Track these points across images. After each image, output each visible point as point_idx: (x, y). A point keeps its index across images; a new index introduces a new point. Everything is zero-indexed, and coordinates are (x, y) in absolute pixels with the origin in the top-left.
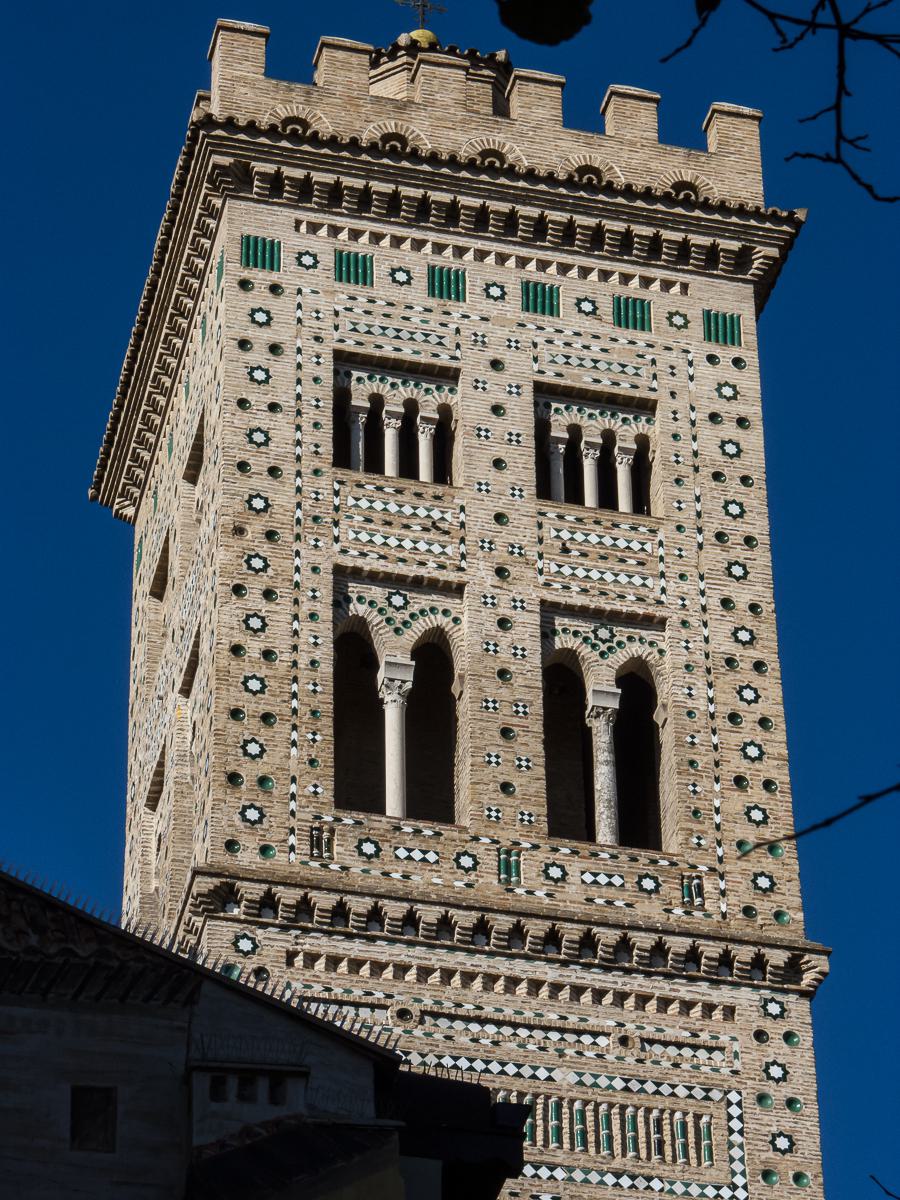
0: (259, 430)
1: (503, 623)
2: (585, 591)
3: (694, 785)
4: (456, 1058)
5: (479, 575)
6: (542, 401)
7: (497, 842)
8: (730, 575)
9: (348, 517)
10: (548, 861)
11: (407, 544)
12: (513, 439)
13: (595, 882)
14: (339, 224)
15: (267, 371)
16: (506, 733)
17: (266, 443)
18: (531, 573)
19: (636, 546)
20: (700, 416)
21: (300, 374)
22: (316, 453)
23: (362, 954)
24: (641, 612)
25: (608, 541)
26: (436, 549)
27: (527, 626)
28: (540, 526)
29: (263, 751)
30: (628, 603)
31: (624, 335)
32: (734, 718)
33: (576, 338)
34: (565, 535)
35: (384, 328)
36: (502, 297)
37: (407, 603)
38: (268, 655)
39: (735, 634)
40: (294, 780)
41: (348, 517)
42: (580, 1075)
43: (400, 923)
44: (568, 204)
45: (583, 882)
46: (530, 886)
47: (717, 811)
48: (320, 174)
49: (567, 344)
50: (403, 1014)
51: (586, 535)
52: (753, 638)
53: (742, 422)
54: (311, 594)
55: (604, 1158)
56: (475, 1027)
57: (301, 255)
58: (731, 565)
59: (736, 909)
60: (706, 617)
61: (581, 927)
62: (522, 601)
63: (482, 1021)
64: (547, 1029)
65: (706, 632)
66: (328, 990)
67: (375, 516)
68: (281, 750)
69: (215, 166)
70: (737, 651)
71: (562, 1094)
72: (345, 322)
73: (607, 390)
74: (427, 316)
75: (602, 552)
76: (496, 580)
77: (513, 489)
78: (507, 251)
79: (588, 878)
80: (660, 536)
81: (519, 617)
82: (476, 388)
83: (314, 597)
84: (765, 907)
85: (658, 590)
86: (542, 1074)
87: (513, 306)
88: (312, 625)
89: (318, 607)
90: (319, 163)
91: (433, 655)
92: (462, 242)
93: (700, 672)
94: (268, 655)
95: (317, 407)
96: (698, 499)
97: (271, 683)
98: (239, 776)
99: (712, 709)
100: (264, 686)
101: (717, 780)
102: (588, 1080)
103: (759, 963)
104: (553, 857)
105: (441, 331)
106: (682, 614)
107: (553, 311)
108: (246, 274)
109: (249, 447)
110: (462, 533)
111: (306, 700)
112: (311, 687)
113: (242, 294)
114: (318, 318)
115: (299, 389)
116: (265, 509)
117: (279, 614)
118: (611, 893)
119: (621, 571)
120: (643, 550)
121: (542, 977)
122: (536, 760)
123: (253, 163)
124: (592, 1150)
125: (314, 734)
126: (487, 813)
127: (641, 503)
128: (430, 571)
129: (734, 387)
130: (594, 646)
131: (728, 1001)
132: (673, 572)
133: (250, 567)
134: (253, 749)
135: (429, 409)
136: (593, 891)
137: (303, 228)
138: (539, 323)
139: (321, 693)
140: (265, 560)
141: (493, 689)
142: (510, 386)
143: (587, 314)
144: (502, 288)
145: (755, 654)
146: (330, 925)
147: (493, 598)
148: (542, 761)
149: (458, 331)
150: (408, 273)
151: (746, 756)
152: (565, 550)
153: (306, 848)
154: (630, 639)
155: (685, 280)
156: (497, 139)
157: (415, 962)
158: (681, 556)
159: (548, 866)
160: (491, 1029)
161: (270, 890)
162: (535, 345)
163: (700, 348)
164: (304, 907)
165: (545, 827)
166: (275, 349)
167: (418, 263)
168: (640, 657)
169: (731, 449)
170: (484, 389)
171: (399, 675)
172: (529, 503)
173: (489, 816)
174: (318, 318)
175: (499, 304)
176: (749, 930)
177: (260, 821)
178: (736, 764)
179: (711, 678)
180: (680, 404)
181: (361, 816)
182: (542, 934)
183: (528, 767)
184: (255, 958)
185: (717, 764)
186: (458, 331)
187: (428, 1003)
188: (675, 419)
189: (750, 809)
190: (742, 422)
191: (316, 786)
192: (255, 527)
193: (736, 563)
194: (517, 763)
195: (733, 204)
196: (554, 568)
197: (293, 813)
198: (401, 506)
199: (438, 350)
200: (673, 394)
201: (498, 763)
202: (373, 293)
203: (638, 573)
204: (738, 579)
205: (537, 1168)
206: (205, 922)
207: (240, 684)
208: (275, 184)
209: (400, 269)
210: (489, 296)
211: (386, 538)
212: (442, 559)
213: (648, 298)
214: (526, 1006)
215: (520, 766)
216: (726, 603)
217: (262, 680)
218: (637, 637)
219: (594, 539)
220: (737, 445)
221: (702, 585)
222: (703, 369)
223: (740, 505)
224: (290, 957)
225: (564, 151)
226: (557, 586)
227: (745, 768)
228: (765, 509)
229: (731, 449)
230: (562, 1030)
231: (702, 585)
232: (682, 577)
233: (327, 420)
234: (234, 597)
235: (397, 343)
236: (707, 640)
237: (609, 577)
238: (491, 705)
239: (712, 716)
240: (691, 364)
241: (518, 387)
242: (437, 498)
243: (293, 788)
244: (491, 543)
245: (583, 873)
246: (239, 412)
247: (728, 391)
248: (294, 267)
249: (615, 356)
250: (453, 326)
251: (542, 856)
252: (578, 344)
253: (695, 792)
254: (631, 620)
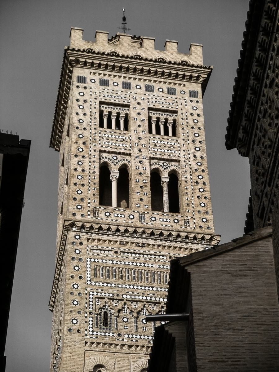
0: (81, 119)
1: (141, 162)
2: (160, 154)
3: (187, 198)
4: (129, 262)
5: (135, 152)
6: (150, 112)
7: (139, 212)
8: (196, 150)
9: (103, 139)
10: (151, 216)
11: (117, 145)
12: (143, 120)
13: (163, 221)
14: (101, 73)
15: (83, 106)
16: (141, 187)
17: (83, 123)
18: (147, 150)
19: (173, 144)
20: (188, 114)
21: (91, 107)
22: (95, 124)
23: (106, 239)
24: (174, 159)
25: (166, 143)
26: (124, 146)
27: (146, 162)
28: (149, 140)
29: (82, 192)
30: (171, 157)
31: (170, 96)
32: (197, 182)
33: (158, 97)
34: (156, 142)
35: (111, 96)
36: (140, 88)
37: (117, 158)
38: (83, 170)
39: (197, 163)
40: (89, 199)
41: (103, 139)
42: (159, 266)
43: (115, 231)
44: (156, 66)
45: (160, 221)
46: (148, 223)
47: (193, 204)
48: (96, 61)
49: (156, 98)
50: (116, 252)
51: (161, 142)
52: (201, 164)
53: (198, 115)
54: (94, 156)
55: (165, 285)
56: (134, 255)
57: (91, 80)
58: (196, 148)
59: (198, 226)
60: (190, 160)
61: (159, 231)
62: (145, 157)
63: (136, 254)
64: (151, 255)
65: (190, 163)
66: (98, 247)
67: (109, 138)
68: (86, 192)
69: (70, 60)
70: (197, 167)
71: (155, 270)
72: (102, 95)
73: (166, 109)
74: (122, 93)
75: (165, 145)
76: (139, 152)
77: (143, 132)
78: (141, 78)
79: (161, 220)
80: (179, 141)
81: (144, 160)
82: (134, 109)
83: (94, 157)
84: (205, 226)
85: (178, 154)
86: (150, 265)
87: (143, 90)
88: (94, 163)
89: (95, 159)
90: (96, 58)
91: (124, 171)
92: (130, 76)
93: (188, 172)
94: (83, 170)
95: (95, 114)
96: (188, 133)
97: (84, 177)
98: (76, 198)
99: (191, 181)
100: (82, 178)
101: (193, 197)
102: (161, 267)
103: (203, 238)
104: (153, 215)
105: (125, 96)
106: (184, 159)
107: (153, 91)
108: (78, 84)
109: (79, 123)
110: (130, 142)
111: (92, 181)
112: (94, 178)
113: (77, 89)
114: (95, 94)
115: (91, 110)
116: (83, 138)
117: (86, 161)
118: (167, 223)
119: (169, 150)
120: (174, 145)
121: (150, 243)
122: (148, 193)
123: (79, 59)
124: (162, 283)
125: (94, 188)
126: (136, 205)
127: (174, 134)
128: (123, 151)
129: (196, 107)
130: (163, 167)
131: (196, 248)
132: (182, 149)
133: (79, 151)
134: (79, 192)
135: (123, 114)
136: (163, 223)
137: (92, 74)
138: (149, 94)
139: (96, 179)
140: (82, 149)
141: (138, 177)
142: (142, 108)
143: (161, 92)
144: (140, 86)
145: (202, 168)
146: (98, 232)
147: (138, 156)
148: (150, 193)
149: (129, 96)
150: (117, 83)
151: (200, 191)
152: (155, 145)
153: (92, 214)
154: (172, 165)
155: (185, 84)
156: (139, 53)
157: (119, 240)
158: (184, 146)
159: (151, 217)
160: (137, 255)
161: (83, 224)
162: (148, 99)
163: (188, 99)
164: (92, 228)
165: (151, 209)
166: (85, 101)
167: (120, 81)
168: (174, 169)
169: (196, 121)
170: (136, 109)
171: (115, 174)
172: (147, 135)
173: (137, 206)
174: (95, 94)
175: (139, 90)
176: (201, 231)
177: (81, 208)
178: (197, 193)
179: (191, 174)
180: (184, 111)
181: (106, 207)
182: (150, 233)
183: (146, 195)
184: (80, 240)
185: (193, 193)
186: (129, 96)
187: (122, 249)
188: (182, 115)
189: (201, 203)
190: (198, 115)
191: (95, 200)
192: (80, 142)
193: (197, 147)
194: (144, 194)
195: (195, 65)
196: (153, 149)
197: (89, 207)
198: (115, 136)
199: (124, 100)
200: (182, 109)
201: (139, 194)
202: (109, 88)
203: (173, 150)
204: (198, 151)
205: (149, 288)
206: (67, 233)
207: (76, 177)
208: (85, 63)
209: (115, 82)
210: (137, 88)
211: (112, 143)
212: (126, 148)
213: (175, 88)
214: (146, 250)
215: (145, 195)
216: (195, 156)
217: (82, 176)
218: (173, 165)
219: (162, 142)
220: (197, 120)
221: (189, 152)
222: (189, 103)
223: (198, 134)
224: (88, 239)
225: (155, 55)
226: (153, 153)
227: (199, 194)
228: (204, 135)
229: (196, 121)
230: (155, 255)
231: (189, 152)
232: (184, 151)
233: (98, 117)
234: (75, 158)
235: (115, 99)
236: (190, 165)
237: (166, 151)
238: (137, 181)
239: (192, 182)
240: (186, 102)
241: (144, 108)
242: (124, 134)
243: (89, 201)
244: (137, 144)
245: (160, 219)
246: (76, 115)
247: (195, 108)
248: (90, 83)
249: (168, 101)
250: (128, 95)
251: (150, 215)
252: (158, 98)
253: (187, 200)
254: (172, 160)
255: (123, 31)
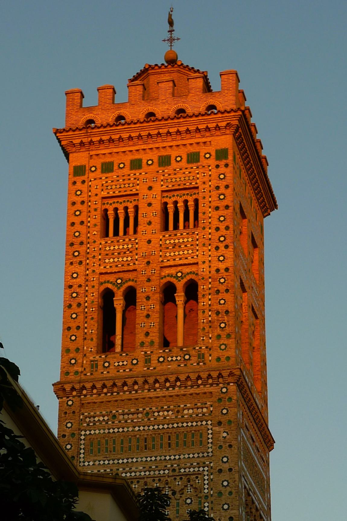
87: (155, 167)
255: (170, 44)
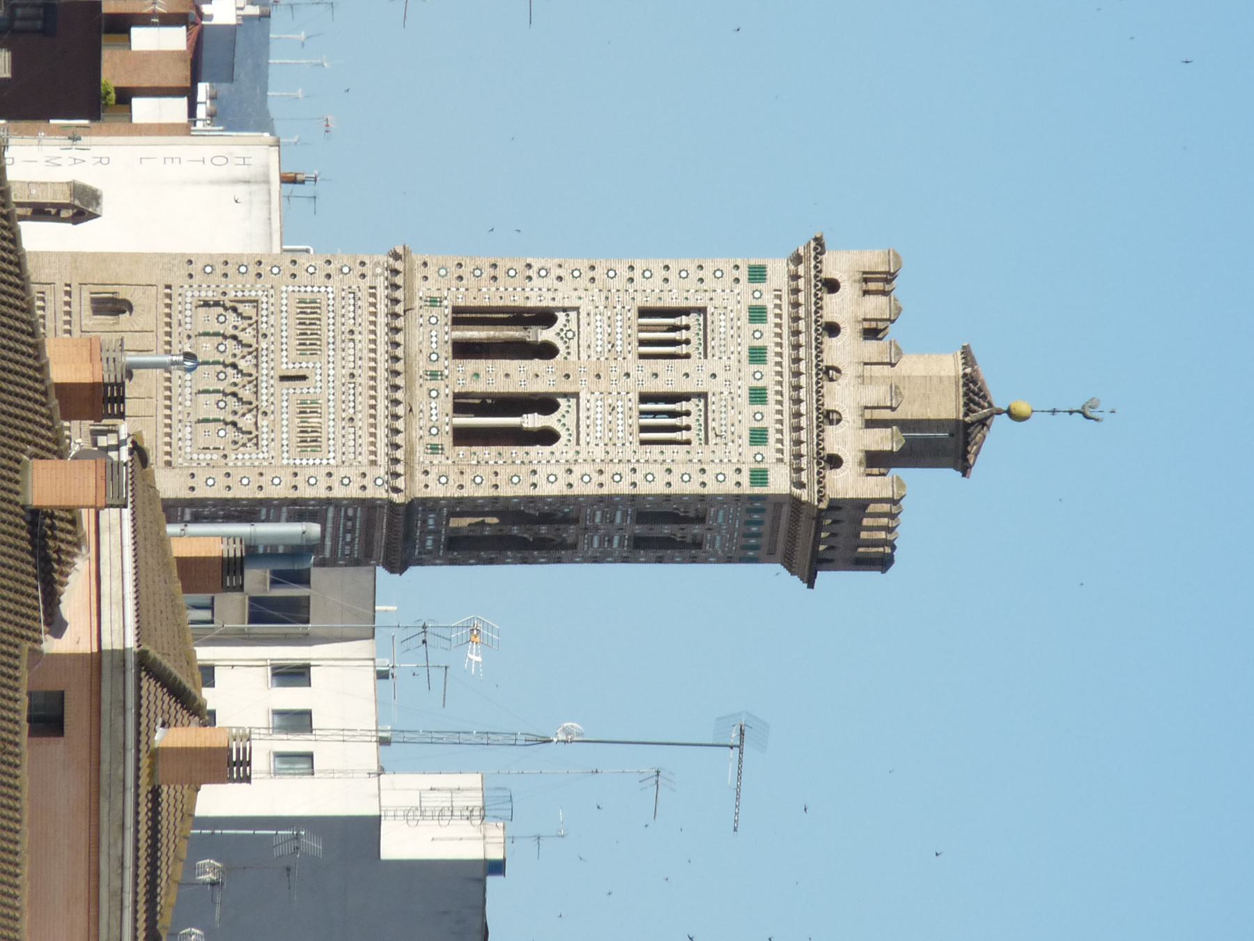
94: (530, 278)
208: (795, 277)
